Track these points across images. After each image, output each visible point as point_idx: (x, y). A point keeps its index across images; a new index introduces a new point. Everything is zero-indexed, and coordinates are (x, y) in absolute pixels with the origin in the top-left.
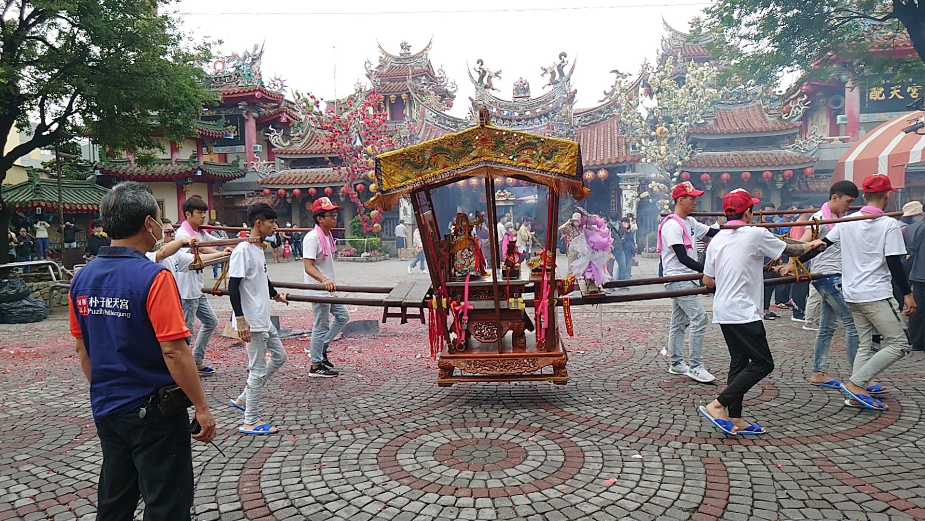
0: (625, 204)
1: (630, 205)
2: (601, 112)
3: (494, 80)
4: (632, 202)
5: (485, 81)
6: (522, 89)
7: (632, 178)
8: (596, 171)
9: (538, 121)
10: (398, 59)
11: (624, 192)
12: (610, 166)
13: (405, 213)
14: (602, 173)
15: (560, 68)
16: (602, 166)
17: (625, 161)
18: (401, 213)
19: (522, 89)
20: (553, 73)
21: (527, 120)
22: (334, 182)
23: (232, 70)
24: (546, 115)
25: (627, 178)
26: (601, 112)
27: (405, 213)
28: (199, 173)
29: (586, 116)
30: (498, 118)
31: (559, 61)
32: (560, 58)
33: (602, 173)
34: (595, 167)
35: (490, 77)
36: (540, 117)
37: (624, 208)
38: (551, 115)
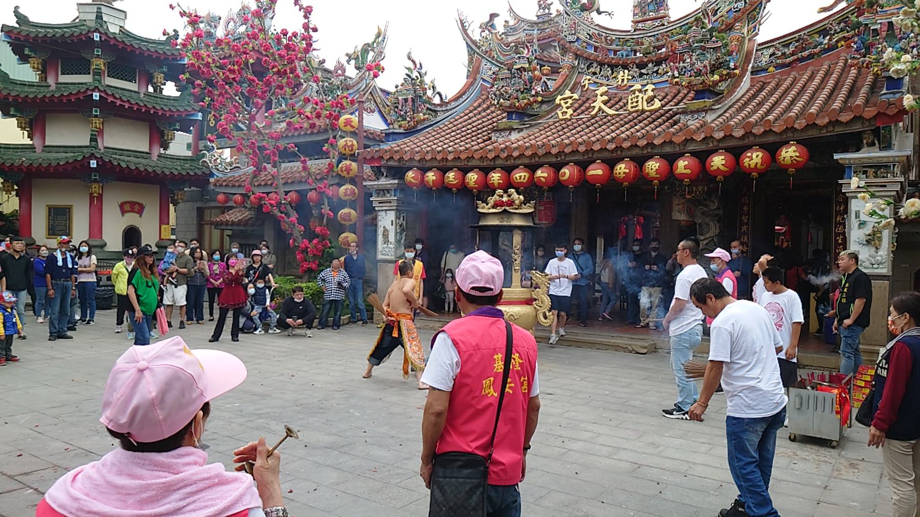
0: (856, 235)
1: (872, 240)
2: (824, 32)
7: (880, 168)
8: (772, 150)
10: (533, 24)
11: (854, 205)
12: (813, 133)
13: (386, 241)
14: (789, 153)
16: (788, 135)
17: (857, 118)
18: (380, 238)
21: (658, 63)
22: (300, 182)
23: (242, 29)
25: (864, 168)
26: (824, 32)
27: (386, 241)
28: (93, 164)
29: (787, 46)
30: (601, 64)
33: (789, 153)
34: (771, 139)
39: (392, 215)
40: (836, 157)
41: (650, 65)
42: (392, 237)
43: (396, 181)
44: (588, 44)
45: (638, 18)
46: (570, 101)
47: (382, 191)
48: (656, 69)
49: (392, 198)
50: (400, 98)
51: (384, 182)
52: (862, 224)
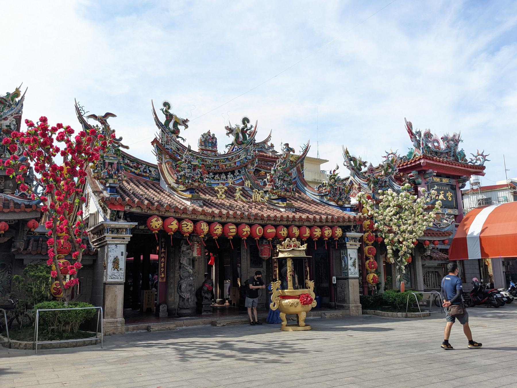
1: (354, 265)
3: (181, 128)
4: (354, 262)
5: (171, 125)
6: (208, 141)
9: (224, 177)
15: (243, 132)
19: (208, 141)
20: (237, 134)
21: (215, 174)
24: (233, 172)
31: (242, 126)
32: (244, 123)
35: (176, 124)
36: (226, 174)
37: (350, 267)
38: (237, 173)
39: (123, 248)
40: (347, 233)
41: (211, 174)
42: (122, 265)
43: (136, 224)
44: (177, 153)
45: (203, 147)
46: (223, 190)
47: (118, 230)
48: (213, 176)
49: (128, 235)
50: (107, 161)
51: (122, 223)
52: (351, 258)
